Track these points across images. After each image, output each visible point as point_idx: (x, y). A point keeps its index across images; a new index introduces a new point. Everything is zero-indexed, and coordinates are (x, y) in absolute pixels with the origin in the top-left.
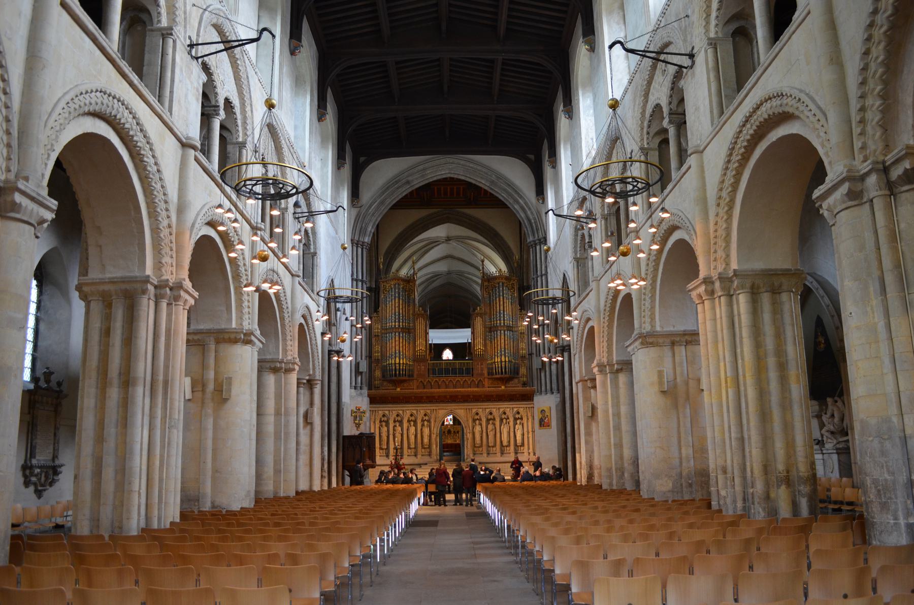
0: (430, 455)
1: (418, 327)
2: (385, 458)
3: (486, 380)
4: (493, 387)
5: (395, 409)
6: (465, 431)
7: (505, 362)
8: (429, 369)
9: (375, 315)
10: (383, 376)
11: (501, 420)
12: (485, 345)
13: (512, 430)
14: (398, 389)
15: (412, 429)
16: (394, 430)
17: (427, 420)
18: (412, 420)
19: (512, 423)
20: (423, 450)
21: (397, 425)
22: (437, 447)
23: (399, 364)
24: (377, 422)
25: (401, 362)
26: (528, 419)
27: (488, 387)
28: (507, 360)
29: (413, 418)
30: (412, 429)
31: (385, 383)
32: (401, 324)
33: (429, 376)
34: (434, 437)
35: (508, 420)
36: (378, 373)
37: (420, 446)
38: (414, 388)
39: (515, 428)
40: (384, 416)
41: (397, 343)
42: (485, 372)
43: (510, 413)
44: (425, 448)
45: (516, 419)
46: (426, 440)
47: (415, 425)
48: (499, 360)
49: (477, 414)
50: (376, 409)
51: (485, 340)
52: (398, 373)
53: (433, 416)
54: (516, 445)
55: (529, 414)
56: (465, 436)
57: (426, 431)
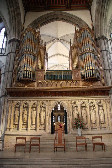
0: (45, 129)
1: (39, 53)
2: (16, 130)
3: (81, 82)
4: (85, 86)
5: (24, 100)
6: (68, 115)
7: (92, 69)
8: (45, 75)
9: (18, 50)
10: (18, 79)
11: (90, 107)
12: (79, 62)
13: (97, 113)
14: (26, 87)
15: (34, 113)
16: (23, 113)
17: (43, 107)
18: (34, 107)
19: (97, 109)
20: (41, 126)
21: (25, 110)
22: (49, 124)
23: (27, 71)
24: (13, 107)
25: (28, 69)
26: (107, 106)
27: (82, 86)
28: (93, 69)
29: (35, 106)
30: (34, 113)
31: (18, 84)
32: (30, 50)
33: (45, 80)
34: (47, 117)
35: (94, 107)
36: (15, 79)
37: (38, 123)
38: (34, 86)
39: (99, 112)
40: (17, 104)
41: (26, 59)
42: (80, 77)
43: (95, 103)
44: (42, 125)
45: (99, 106)
46: (43, 120)
47: (36, 110)
48: (88, 69)
49: (75, 103)
50: (13, 100)
51: (79, 60)
52: (25, 76)
53: (47, 105)
54: (100, 122)
55: (107, 103)
56: (68, 118)
57: (43, 114)
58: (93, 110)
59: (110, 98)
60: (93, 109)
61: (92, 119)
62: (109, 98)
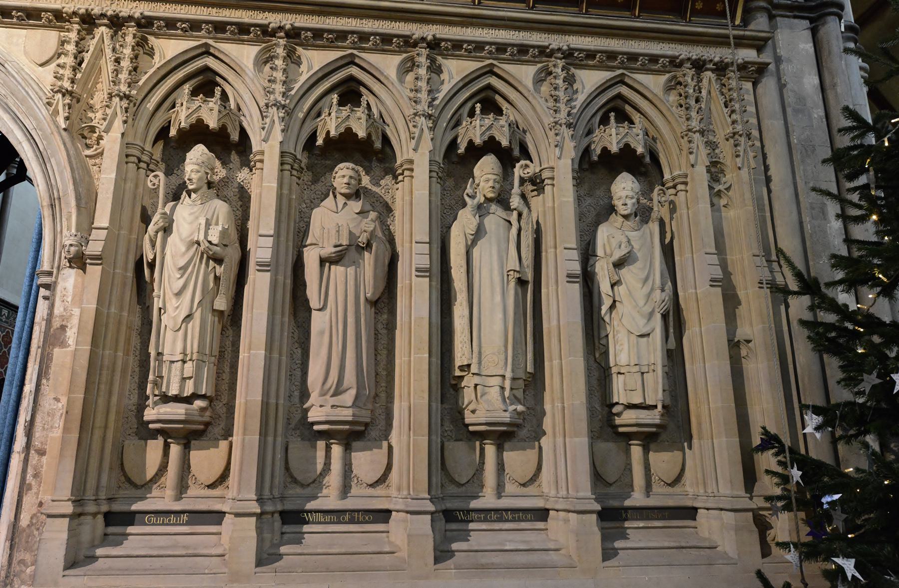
39: (587, 253)
58: (496, 214)
59: (766, 57)
60: (502, 200)
61: (461, 354)
62: (748, 55)
